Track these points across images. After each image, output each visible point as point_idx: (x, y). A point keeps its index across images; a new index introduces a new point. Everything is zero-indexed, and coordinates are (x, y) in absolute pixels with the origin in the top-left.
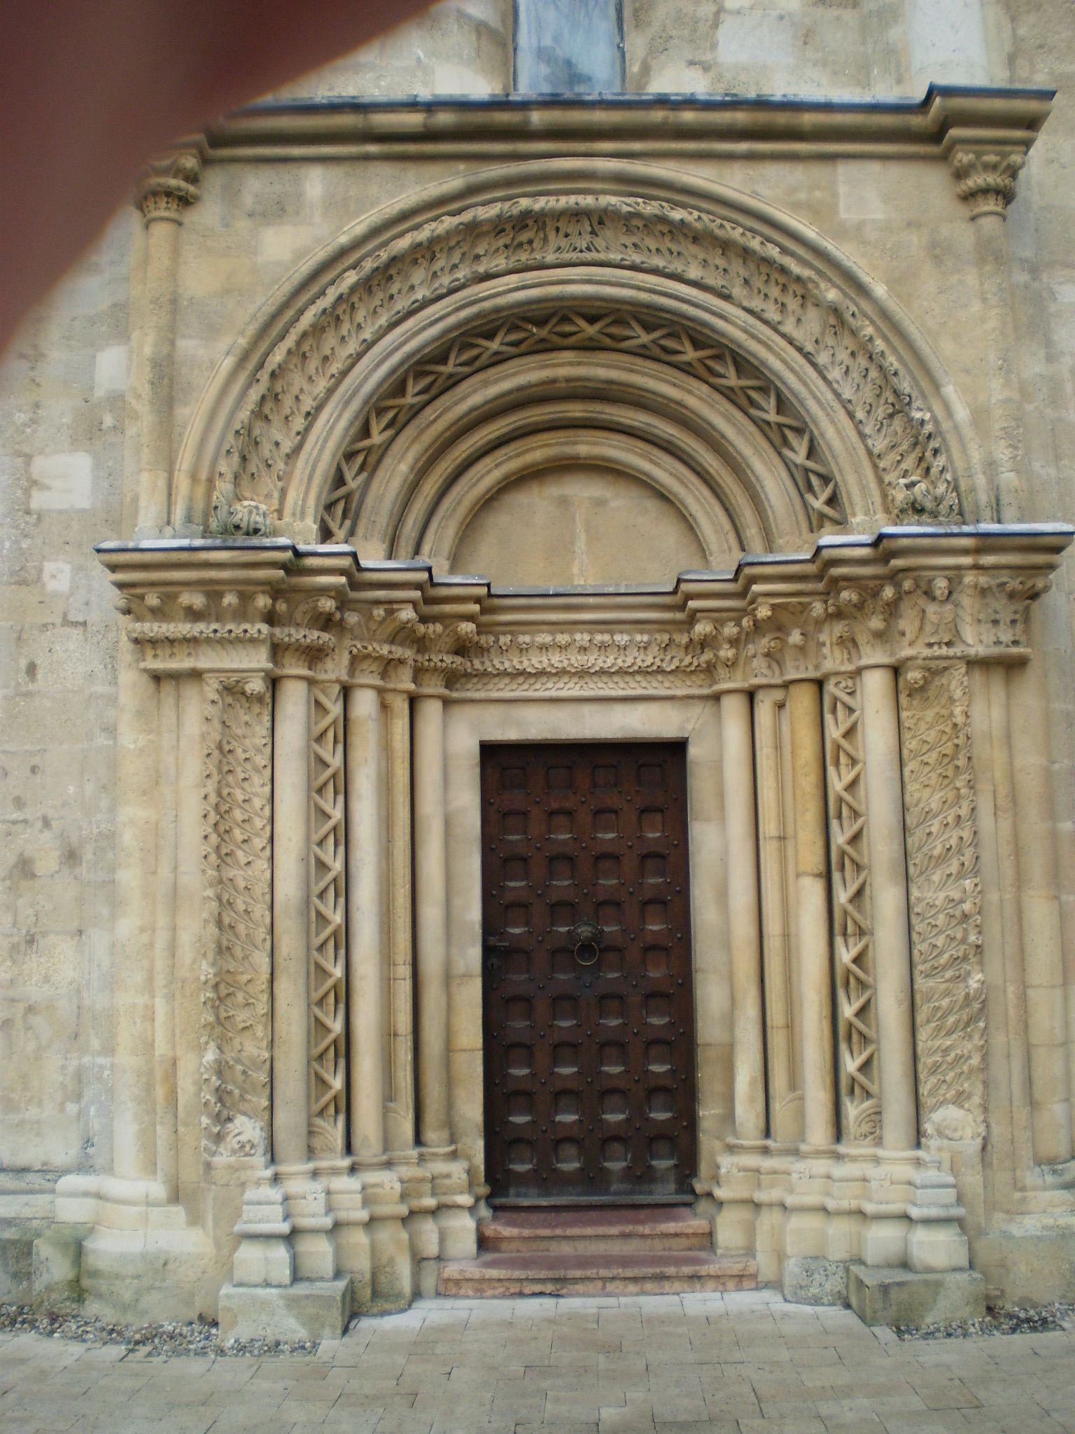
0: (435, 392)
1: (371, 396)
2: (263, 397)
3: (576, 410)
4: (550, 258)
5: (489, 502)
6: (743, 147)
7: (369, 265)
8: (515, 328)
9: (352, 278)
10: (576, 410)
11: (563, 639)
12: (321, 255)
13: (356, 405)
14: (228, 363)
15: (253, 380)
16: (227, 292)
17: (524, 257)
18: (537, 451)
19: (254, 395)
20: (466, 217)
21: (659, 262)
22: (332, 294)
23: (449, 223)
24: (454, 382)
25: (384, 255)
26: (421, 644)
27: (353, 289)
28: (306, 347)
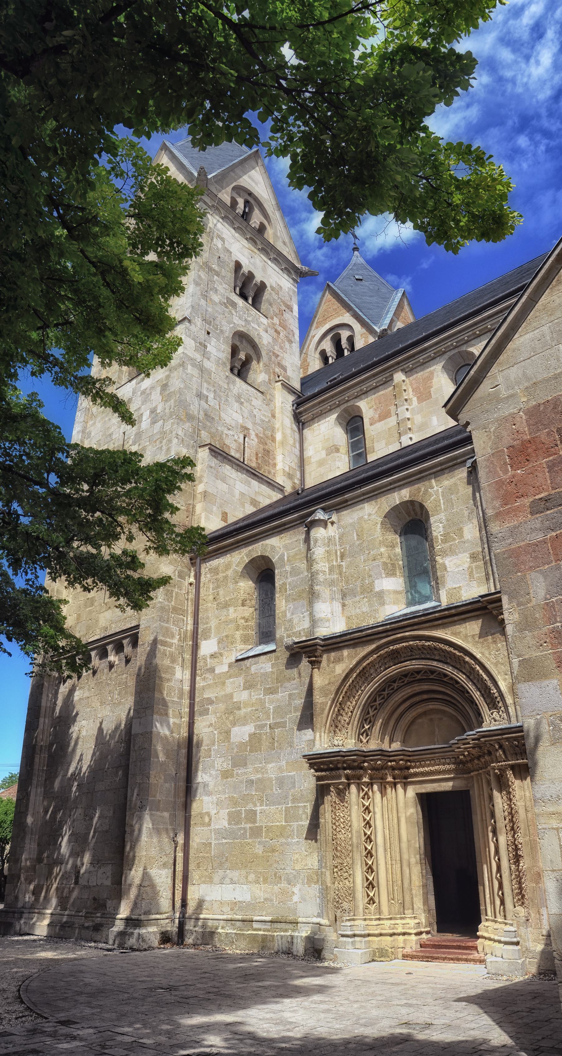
0: (386, 699)
1: (365, 704)
2: (339, 710)
3: (425, 696)
4: (402, 660)
5: (412, 722)
6: (440, 622)
7: (358, 671)
8: (400, 679)
9: (355, 675)
10: (425, 696)
11: (432, 762)
12: (347, 671)
13: (361, 708)
14: (329, 702)
15: (336, 706)
16: (329, 683)
17: (396, 661)
18: (420, 709)
19: (336, 709)
20: (379, 654)
21: (428, 656)
22: (351, 680)
23: (375, 656)
24: (389, 696)
25: (361, 668)
26: (393, 768)
27: (356, 678)
28: (348, 694)
